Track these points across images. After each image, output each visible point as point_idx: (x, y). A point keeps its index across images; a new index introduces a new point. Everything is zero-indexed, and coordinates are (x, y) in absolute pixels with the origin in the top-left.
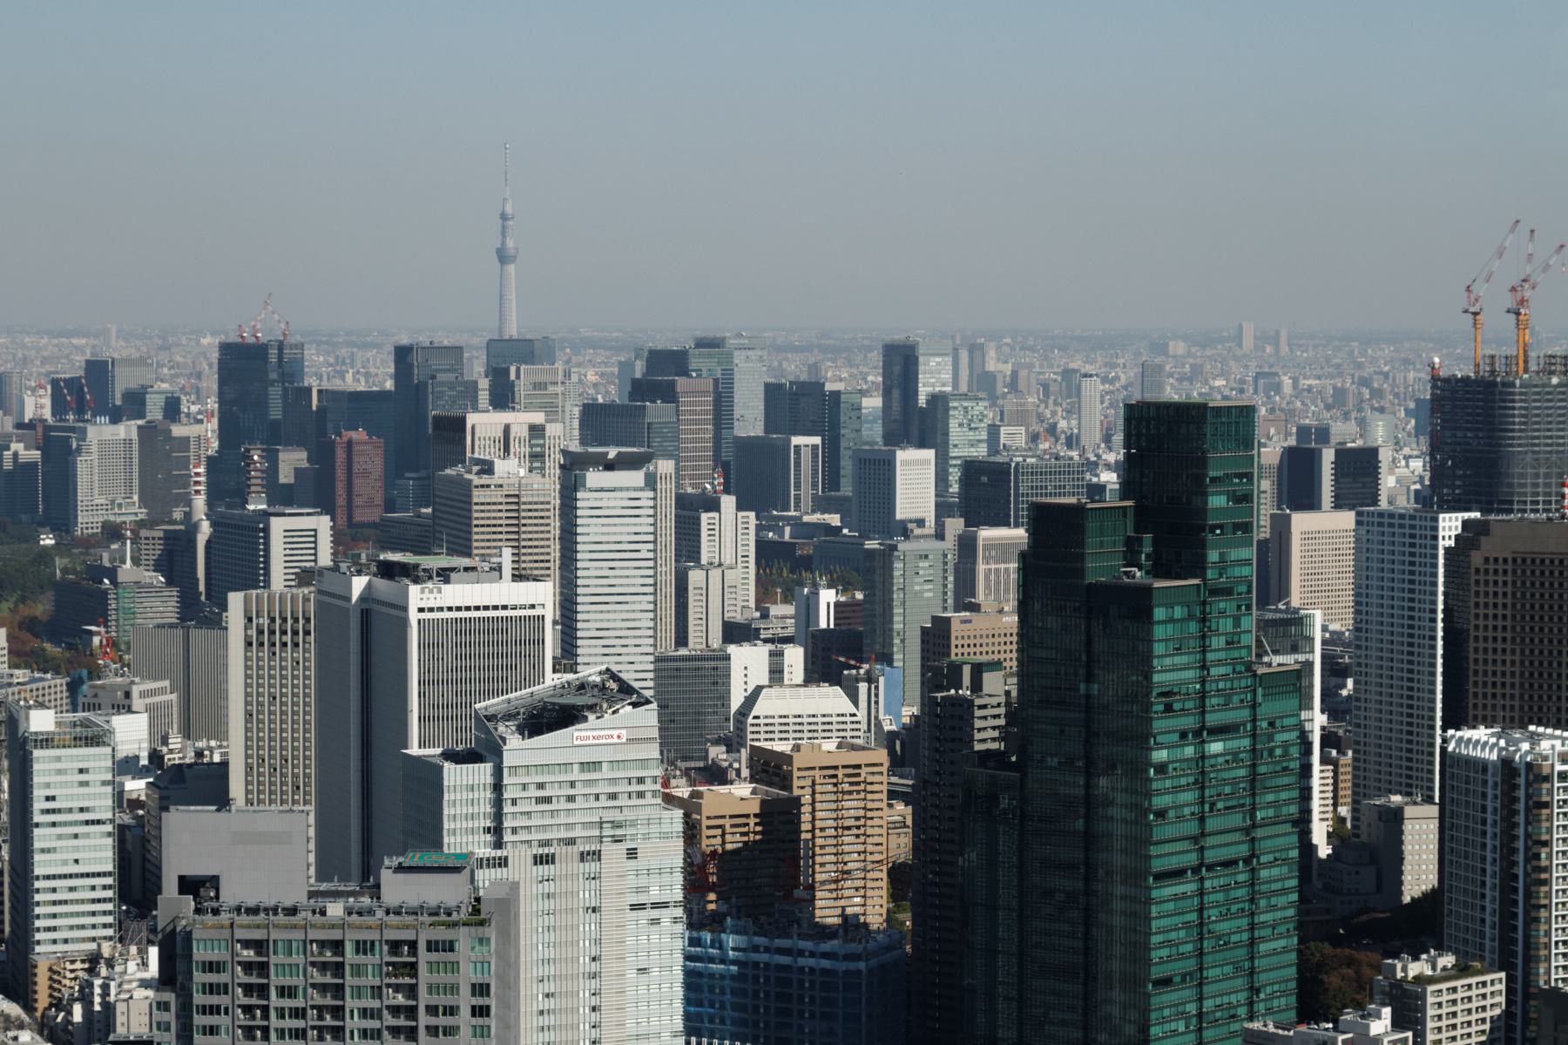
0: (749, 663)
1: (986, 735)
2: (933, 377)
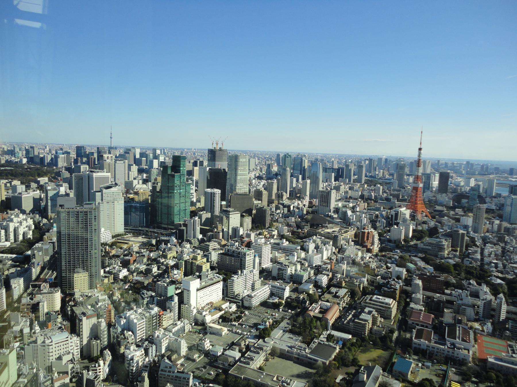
0: (135, 182)
1: (158, 190)
2: (158, 152)
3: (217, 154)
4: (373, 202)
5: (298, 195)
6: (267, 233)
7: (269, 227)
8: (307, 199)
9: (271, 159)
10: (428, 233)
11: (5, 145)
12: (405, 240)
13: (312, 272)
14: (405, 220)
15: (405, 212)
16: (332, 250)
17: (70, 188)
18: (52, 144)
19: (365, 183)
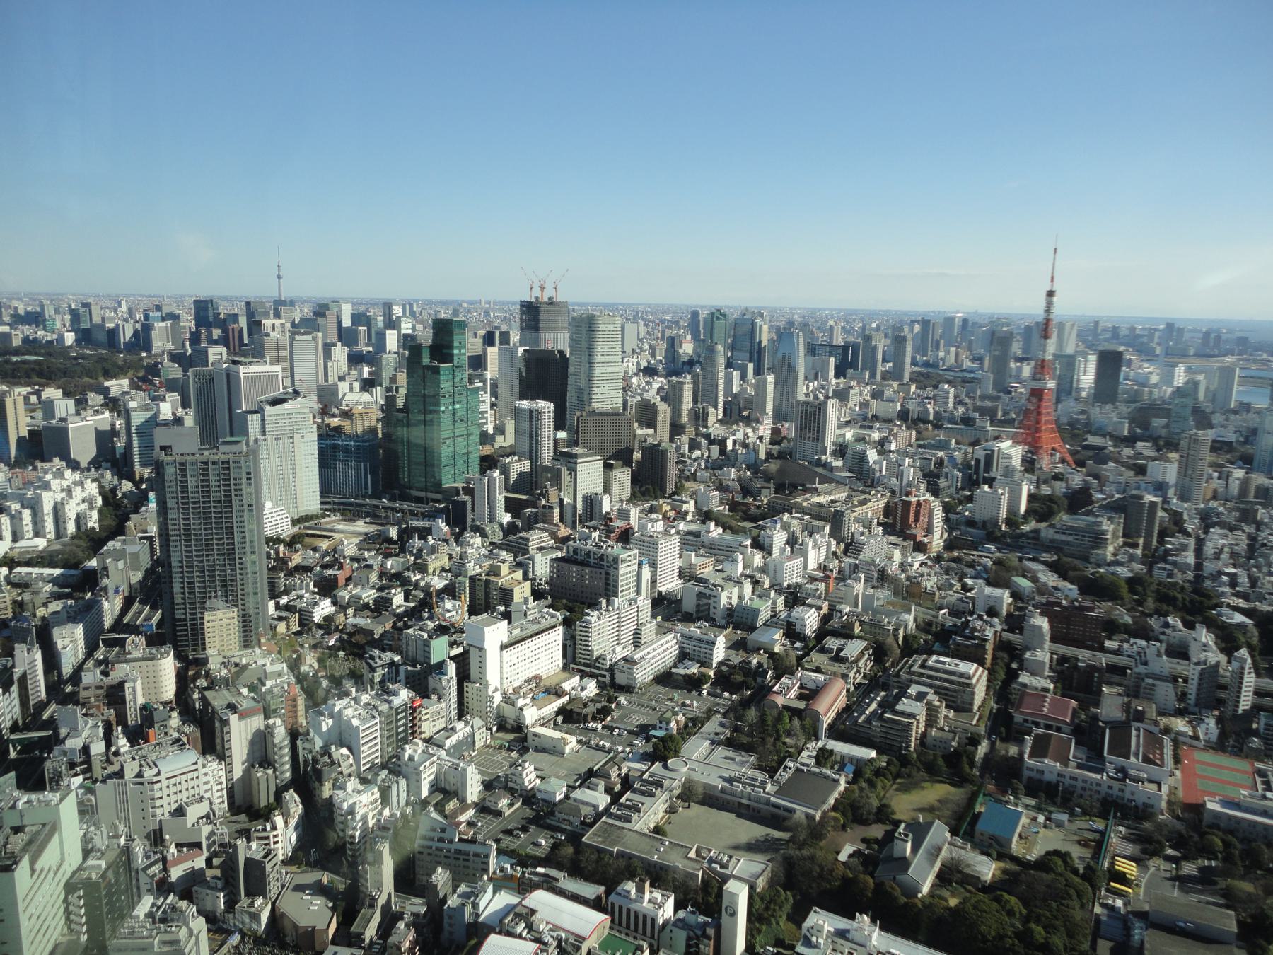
0: (343, 387)
1: (400, 405)
2: (397, 311)
3: (543, 312)
4: (930, 427)
5: (746, 413)
6: (669, 508)
7: (674, 493)
8: (768, 421)
9: (677, 323)
10: (1066, 502)
11: (20, 299)
12: (1008, 521)
13: (781, 600)
14: (1009, 472)
15: (1011, 451)
16: (828, 546)
17: (185, 405)
18: (134, 296)
19: (911, 380)
